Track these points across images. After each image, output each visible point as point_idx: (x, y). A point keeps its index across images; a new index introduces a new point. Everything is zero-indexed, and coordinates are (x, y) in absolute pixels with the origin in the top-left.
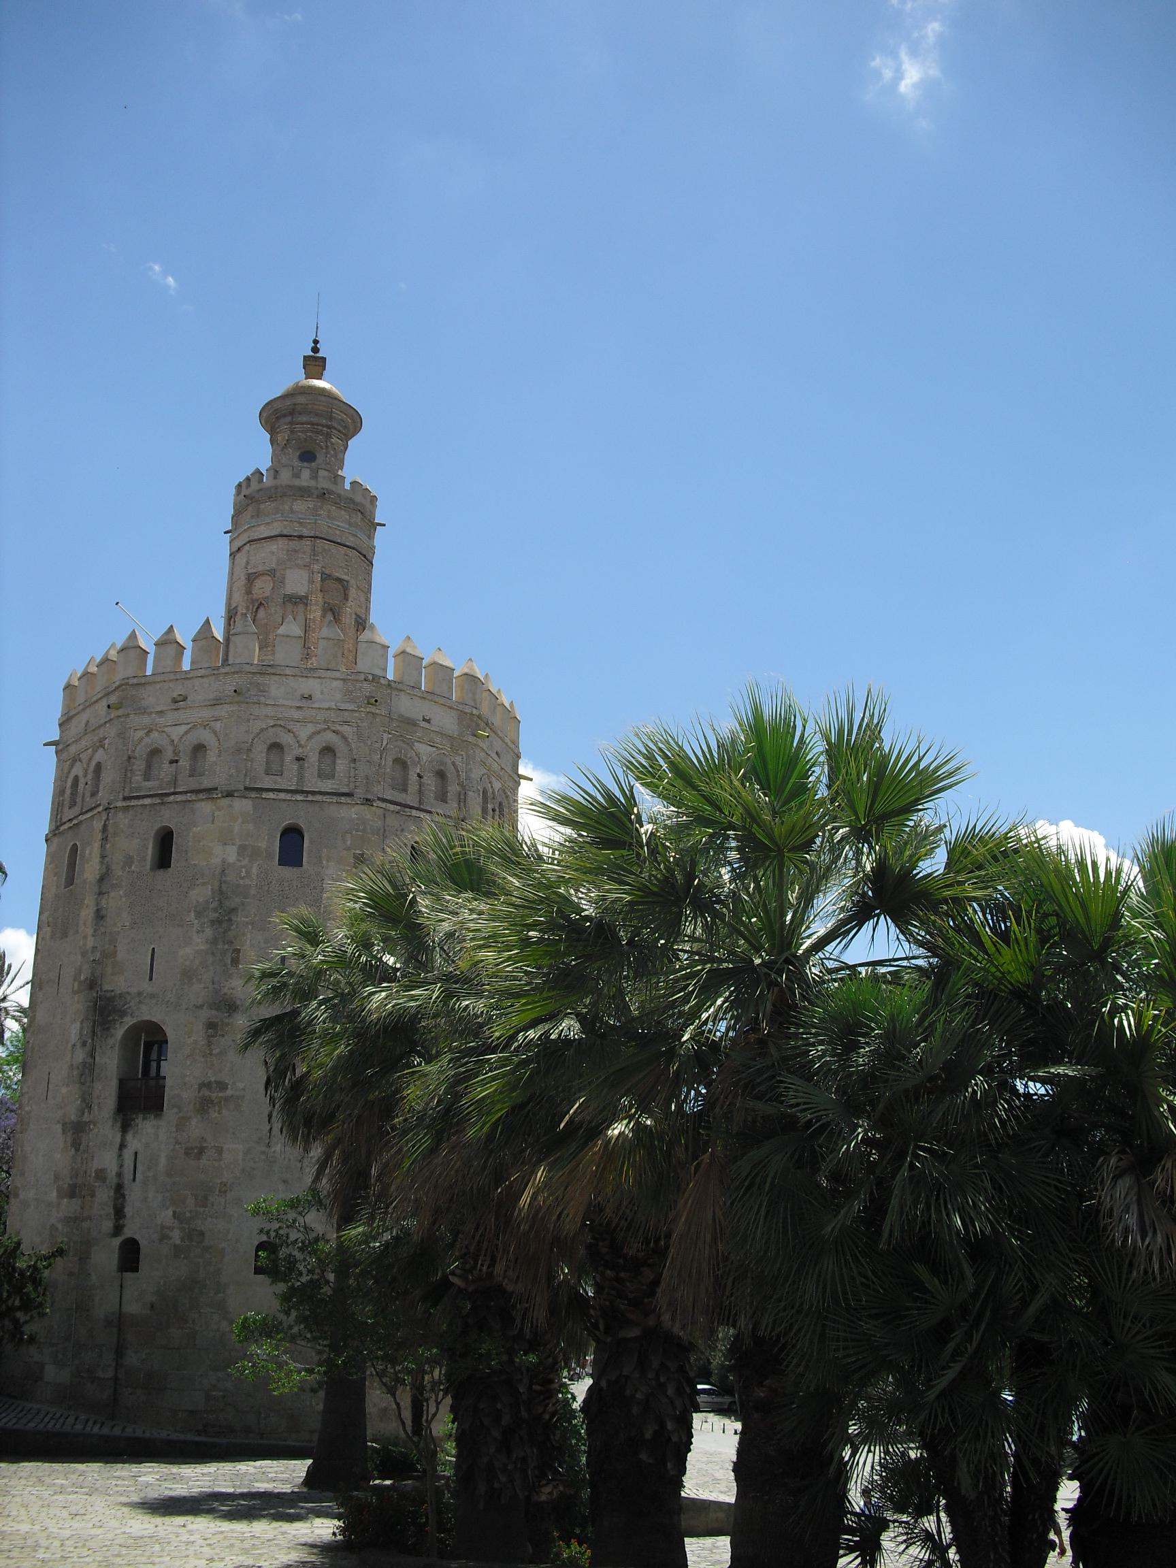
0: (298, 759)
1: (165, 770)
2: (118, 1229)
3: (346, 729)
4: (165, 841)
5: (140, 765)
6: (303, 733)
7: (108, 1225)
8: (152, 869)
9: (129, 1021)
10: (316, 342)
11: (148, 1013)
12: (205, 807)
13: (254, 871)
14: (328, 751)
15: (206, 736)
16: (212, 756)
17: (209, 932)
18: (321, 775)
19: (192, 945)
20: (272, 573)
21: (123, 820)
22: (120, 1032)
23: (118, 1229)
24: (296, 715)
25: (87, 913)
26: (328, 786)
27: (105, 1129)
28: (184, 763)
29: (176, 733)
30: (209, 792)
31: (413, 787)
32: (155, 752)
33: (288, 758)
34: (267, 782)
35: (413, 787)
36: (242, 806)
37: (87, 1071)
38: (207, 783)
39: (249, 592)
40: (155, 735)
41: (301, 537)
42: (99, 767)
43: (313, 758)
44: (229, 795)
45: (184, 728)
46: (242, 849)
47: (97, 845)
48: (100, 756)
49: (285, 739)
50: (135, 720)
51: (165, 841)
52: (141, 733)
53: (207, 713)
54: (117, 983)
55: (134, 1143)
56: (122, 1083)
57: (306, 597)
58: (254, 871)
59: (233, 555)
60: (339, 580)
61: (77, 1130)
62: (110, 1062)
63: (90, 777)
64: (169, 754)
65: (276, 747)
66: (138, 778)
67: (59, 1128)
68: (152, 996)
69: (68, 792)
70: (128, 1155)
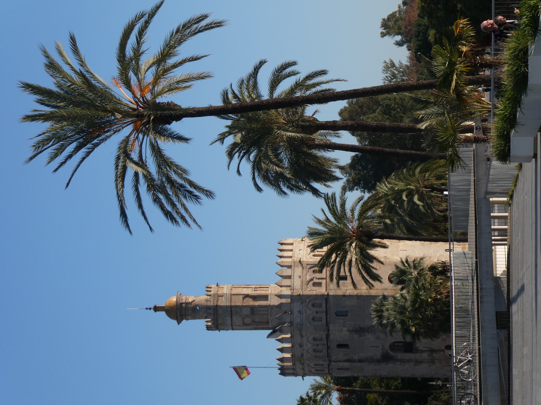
0: (317, 313)
1: (320, 348)
2: (443, 351)
3: (307, 301)
4: (340, 346)
5: (318, 354)
6: (309, 312)
7: (442, 353)
8: (348, 348)
9: (389, 351)
10: (147, 309)
11: (387, 347)
12: (332, 337)
13: (349, 323)
14: (313, 305)
15: (311, 338)
16: (317, 336)
17: (366, 334)
18: (321, 306)
19: (370, 337)
20: (243, 319)
21: (334, 358)
22: (392, 353)
23: (443, 351)
24: (304, 315)
25: (359, 364)
26: (324, 305)
27: (418, 356)
28: (318, 342)
29: (309, 345)
30: (328, 336)
31: (320, 281)
32: (314, 350)
33: (317, 315)
34: (324, 321)
35: (320, 281)
36: (331, 327)
37: (403, 361)
38: (324, 336)
39: (249, 325)
40: (309, 351)
41: (231, 311)
42: (315, 365)
43: (316, 309)
44: (328, 330)
45: (309, 344)
46: (344, 326)
47: (340, 363)
48: (312, 365)
49: (311, 317)
50: (305, 356)
51: (340, 346)
52: (309, 355)
53: (305, 338)
54: (378, 354)
55: (421, 348)
56: (405, 352)
57: (251, 308)
58: (349, 323)
59: (233, 329)
60: (244, 298)
61: (418, 362)
62: (400, 355)
63: (317, 367)
64: (315, 347)
65: (313, 319)
66: (322, 354)
67: (416, 367)
68: (383, 346)
69: (319, 372)
70: (424, 349)
